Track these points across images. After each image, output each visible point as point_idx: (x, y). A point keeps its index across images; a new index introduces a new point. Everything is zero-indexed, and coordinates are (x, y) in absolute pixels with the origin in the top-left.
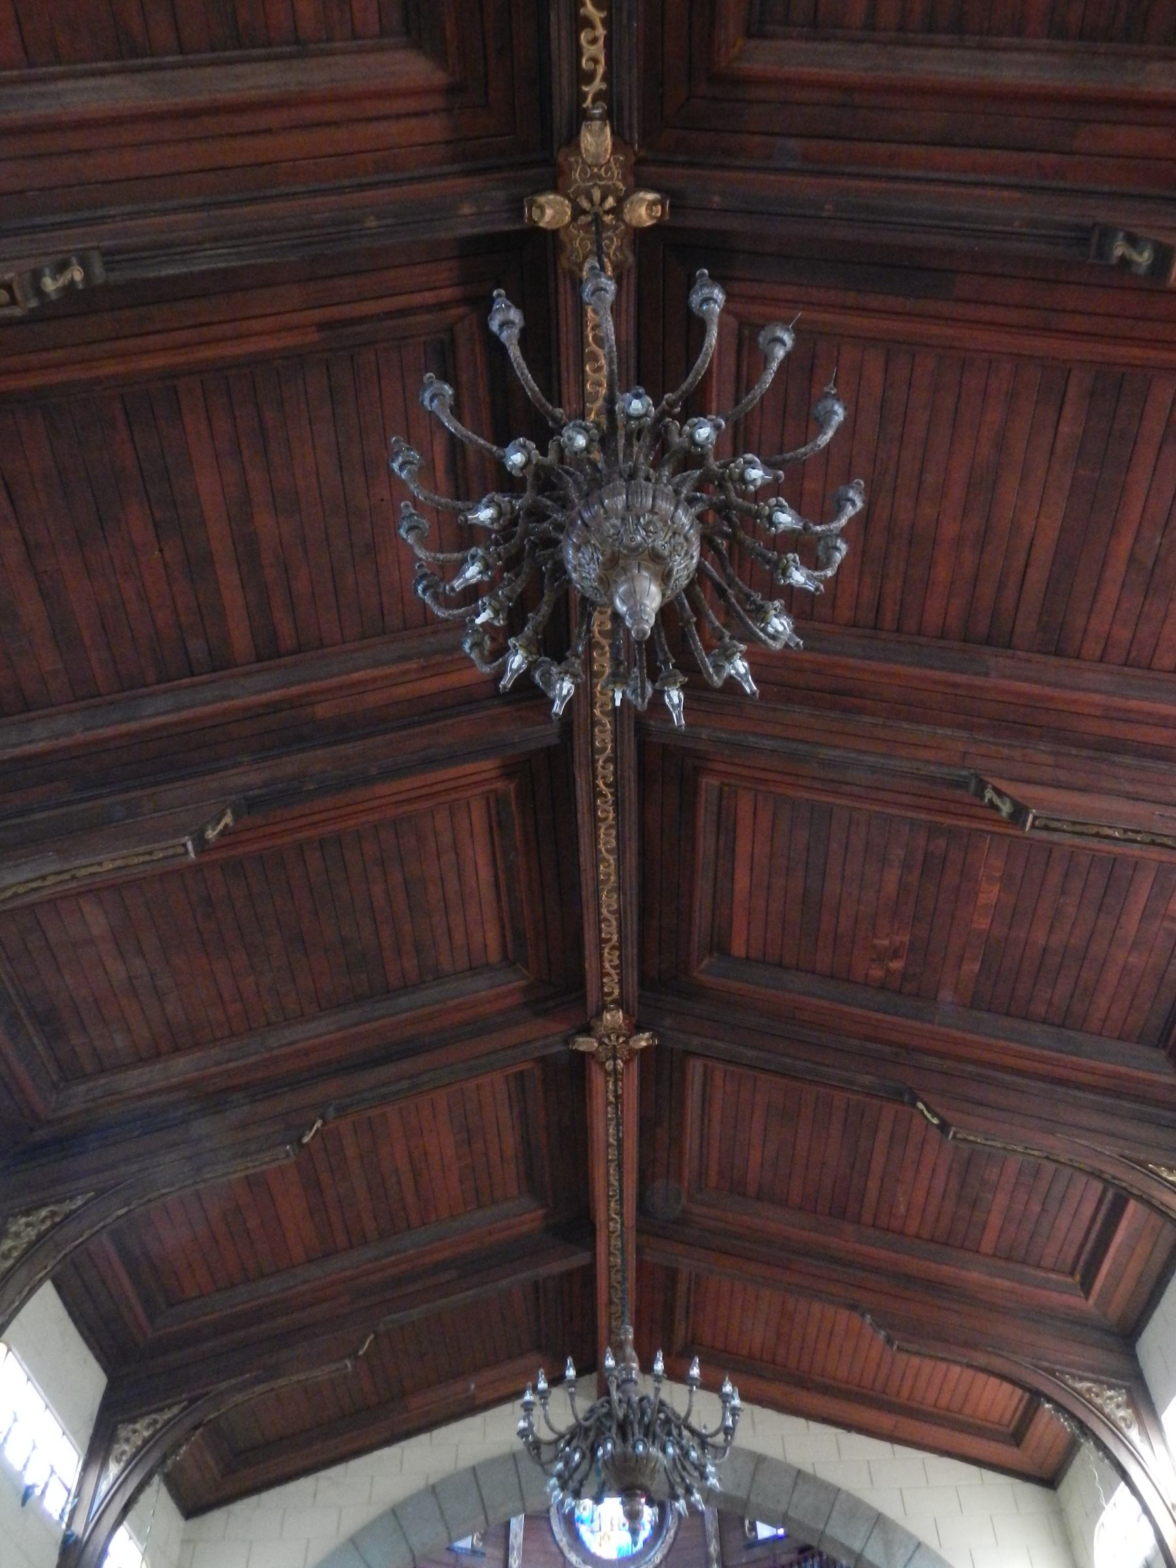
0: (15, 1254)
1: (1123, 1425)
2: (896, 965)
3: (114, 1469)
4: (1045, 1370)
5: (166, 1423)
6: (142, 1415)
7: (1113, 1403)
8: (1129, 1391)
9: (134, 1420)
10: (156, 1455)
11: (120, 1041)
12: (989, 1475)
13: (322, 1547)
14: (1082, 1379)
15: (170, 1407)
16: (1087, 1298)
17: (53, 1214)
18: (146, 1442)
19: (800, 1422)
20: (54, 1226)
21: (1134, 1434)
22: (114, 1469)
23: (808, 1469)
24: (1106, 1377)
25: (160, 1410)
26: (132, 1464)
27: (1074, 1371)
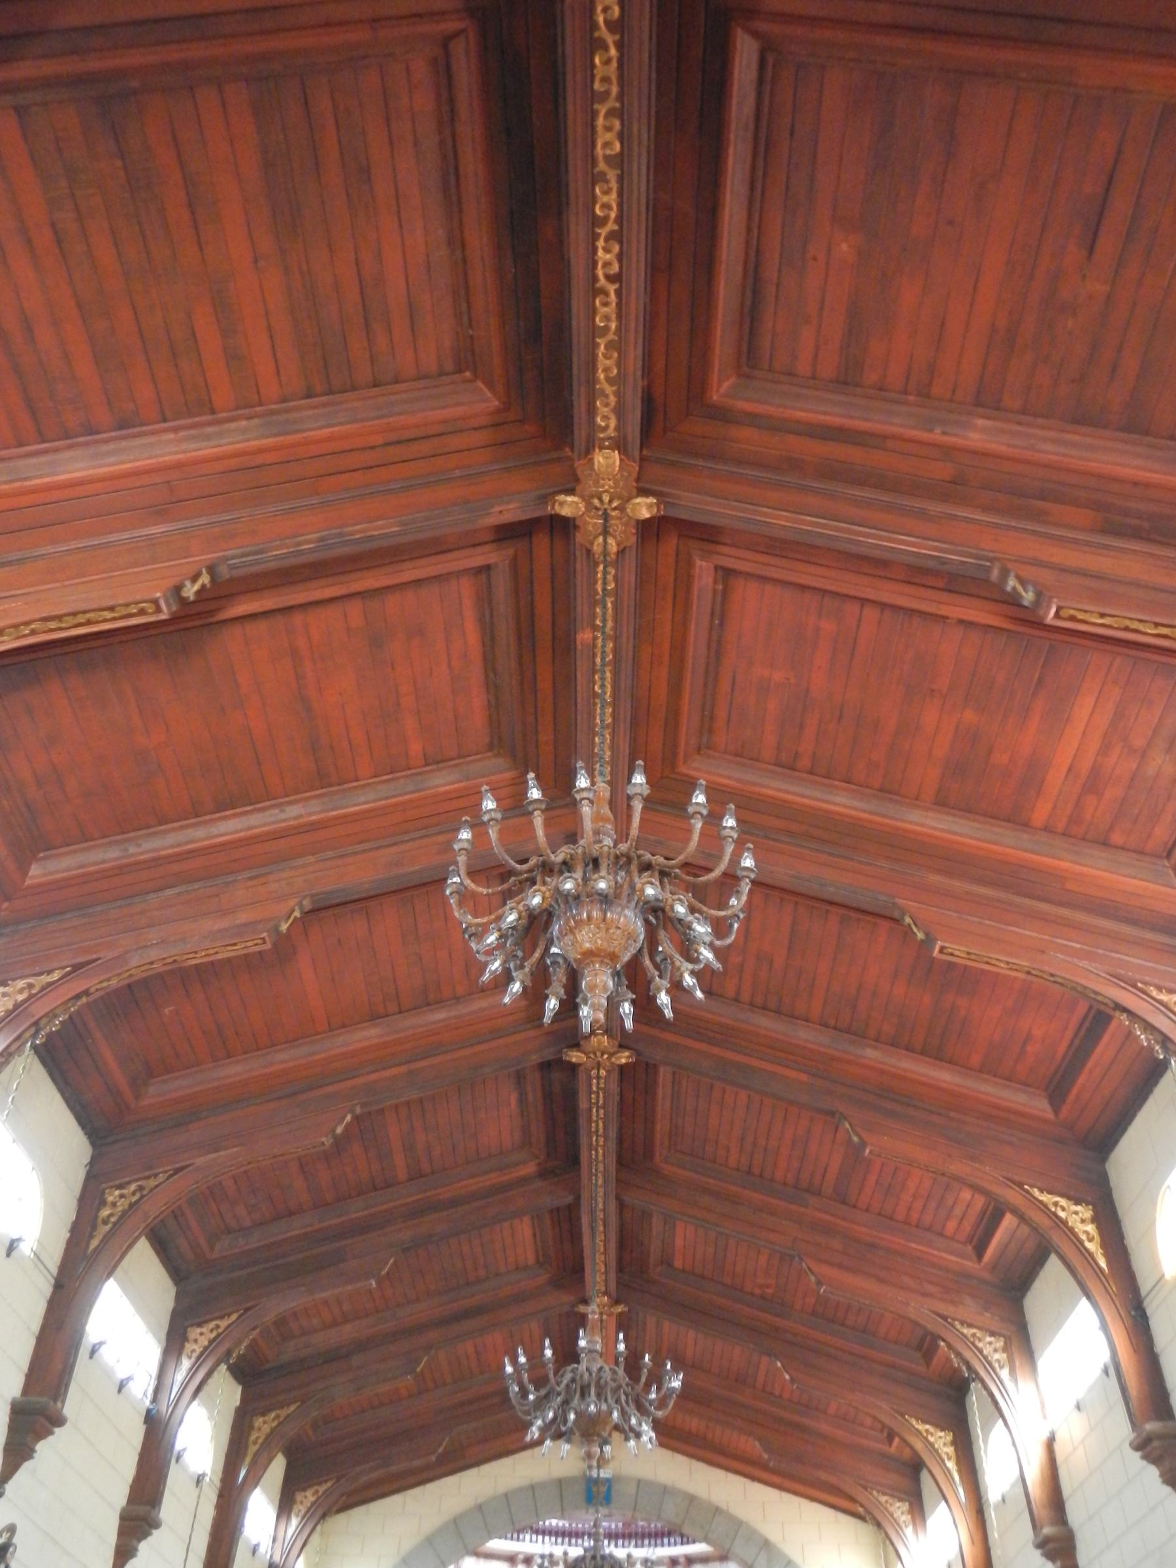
0: (260, 1441)
1: (903, 1526)
2: (770, 1291)
3: (294, 1522)
4: (861, 1485)
5: (325, 1492)
6: (310, 1486)
7: (900, 1510)
8: (911, 1505)
9: (304, 1490)
10: (320, 1512)
11: (315, 1321)
12: (842, 1517)
13: (409, 1544)
14: (884, 1494)
15: (326, 1482)
16: (890, 1443)
17: (278, 1417)
18: (313, 1504)
19: (721, 1473)
20: (280, 1424)
21: (909, 1531)
22: (294, 1522)
23: (723, 1506)
24: (898, 1493)
25: (320, 1484)
26: (306, 1517)
27: (879, 1488)
